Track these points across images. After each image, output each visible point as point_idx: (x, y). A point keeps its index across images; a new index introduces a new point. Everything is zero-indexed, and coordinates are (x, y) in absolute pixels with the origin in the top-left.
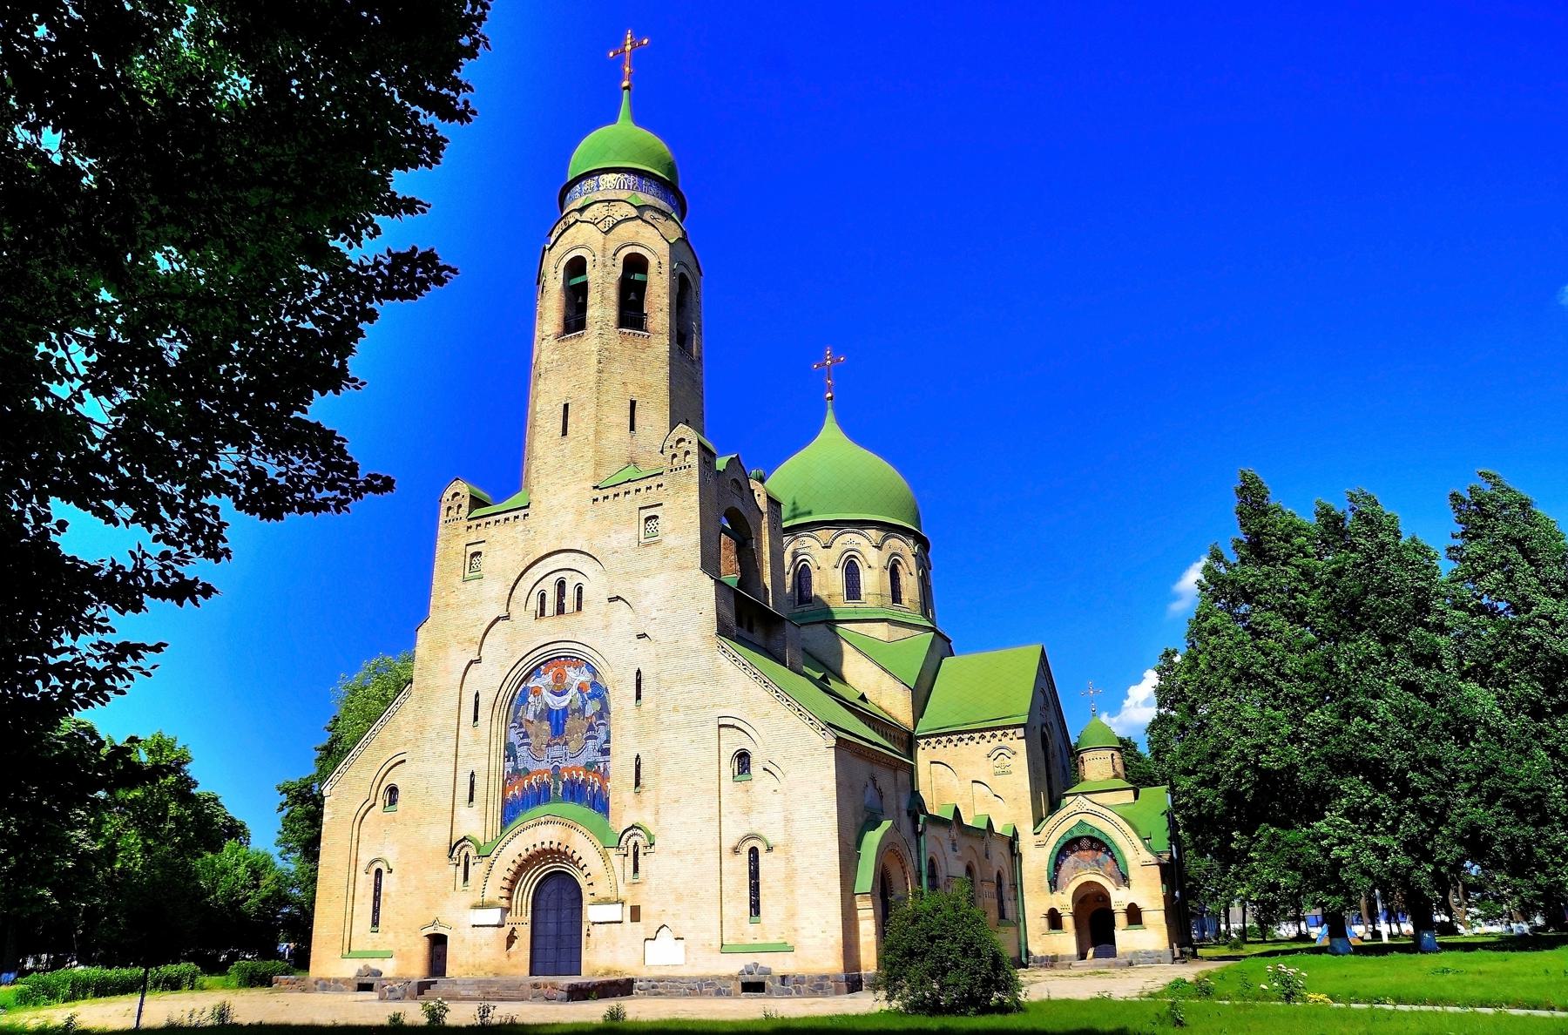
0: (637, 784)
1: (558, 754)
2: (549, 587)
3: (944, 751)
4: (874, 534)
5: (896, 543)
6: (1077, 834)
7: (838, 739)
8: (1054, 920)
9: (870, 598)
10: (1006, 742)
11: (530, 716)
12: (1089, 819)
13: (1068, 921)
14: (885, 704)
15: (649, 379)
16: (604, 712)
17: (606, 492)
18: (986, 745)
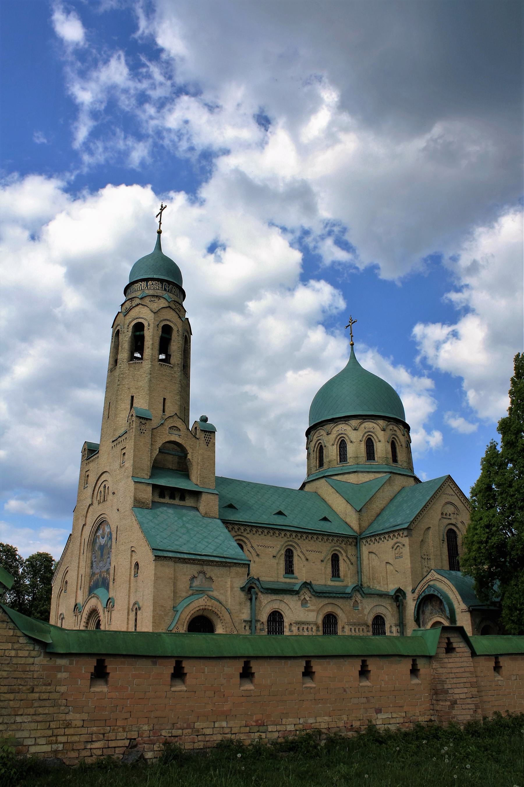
0: (114, 580)
1: (101, 565)
2: (102, 489)
3: (375, 547)
4: (354, 423)
5: (369, 425)
6: (427, 593)
7: (156, 556)
9: (351, 460)
11: (97, 549)
12: (439, 585)
14: (348, 520)
15: (140, 384)
16: (111, 545)
17: (115, 443)
18: (391, 542)
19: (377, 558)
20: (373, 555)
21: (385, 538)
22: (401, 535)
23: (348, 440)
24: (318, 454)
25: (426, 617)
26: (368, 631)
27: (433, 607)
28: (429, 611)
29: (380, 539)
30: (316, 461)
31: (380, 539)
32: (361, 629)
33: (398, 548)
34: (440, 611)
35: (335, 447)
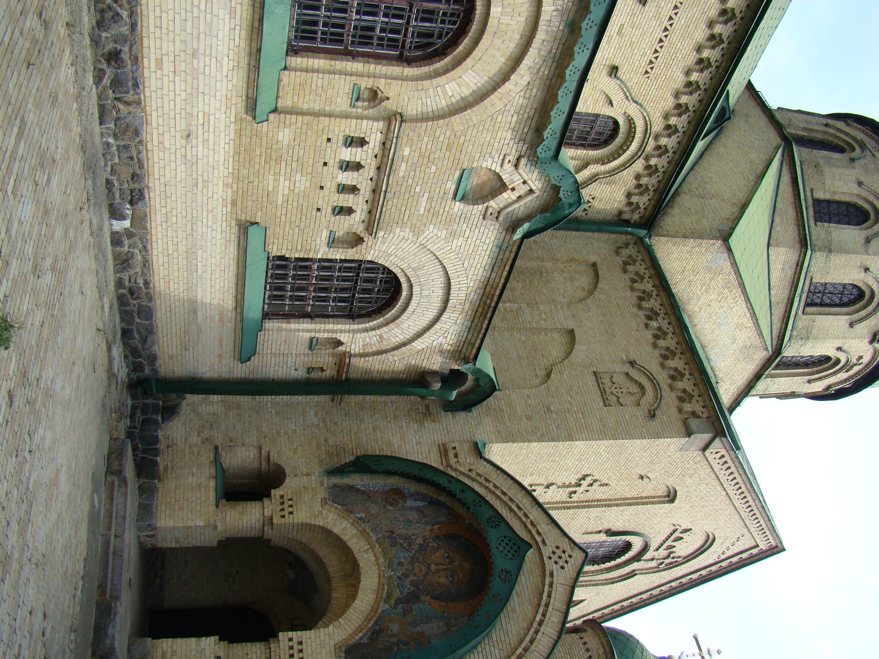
8: (251, 486)
9: (823, 235)
10: (670, 399)
13: (246, 518)
18: (650, 359)
19: (580, 294)
20: (584, 280)
21: (659, 334)
22: (687, 407)
23: (870, 232)
24: (819, 136)
25: (374, 509)
26: (333, 242)
27: (423, 548)
28: (401, 530)
29: (652, 315)
30: (805, 129)
31: (652, 315)
32: (347, 200)
33: (635, 389)
34: (408, 588)
35: (855, 189)
